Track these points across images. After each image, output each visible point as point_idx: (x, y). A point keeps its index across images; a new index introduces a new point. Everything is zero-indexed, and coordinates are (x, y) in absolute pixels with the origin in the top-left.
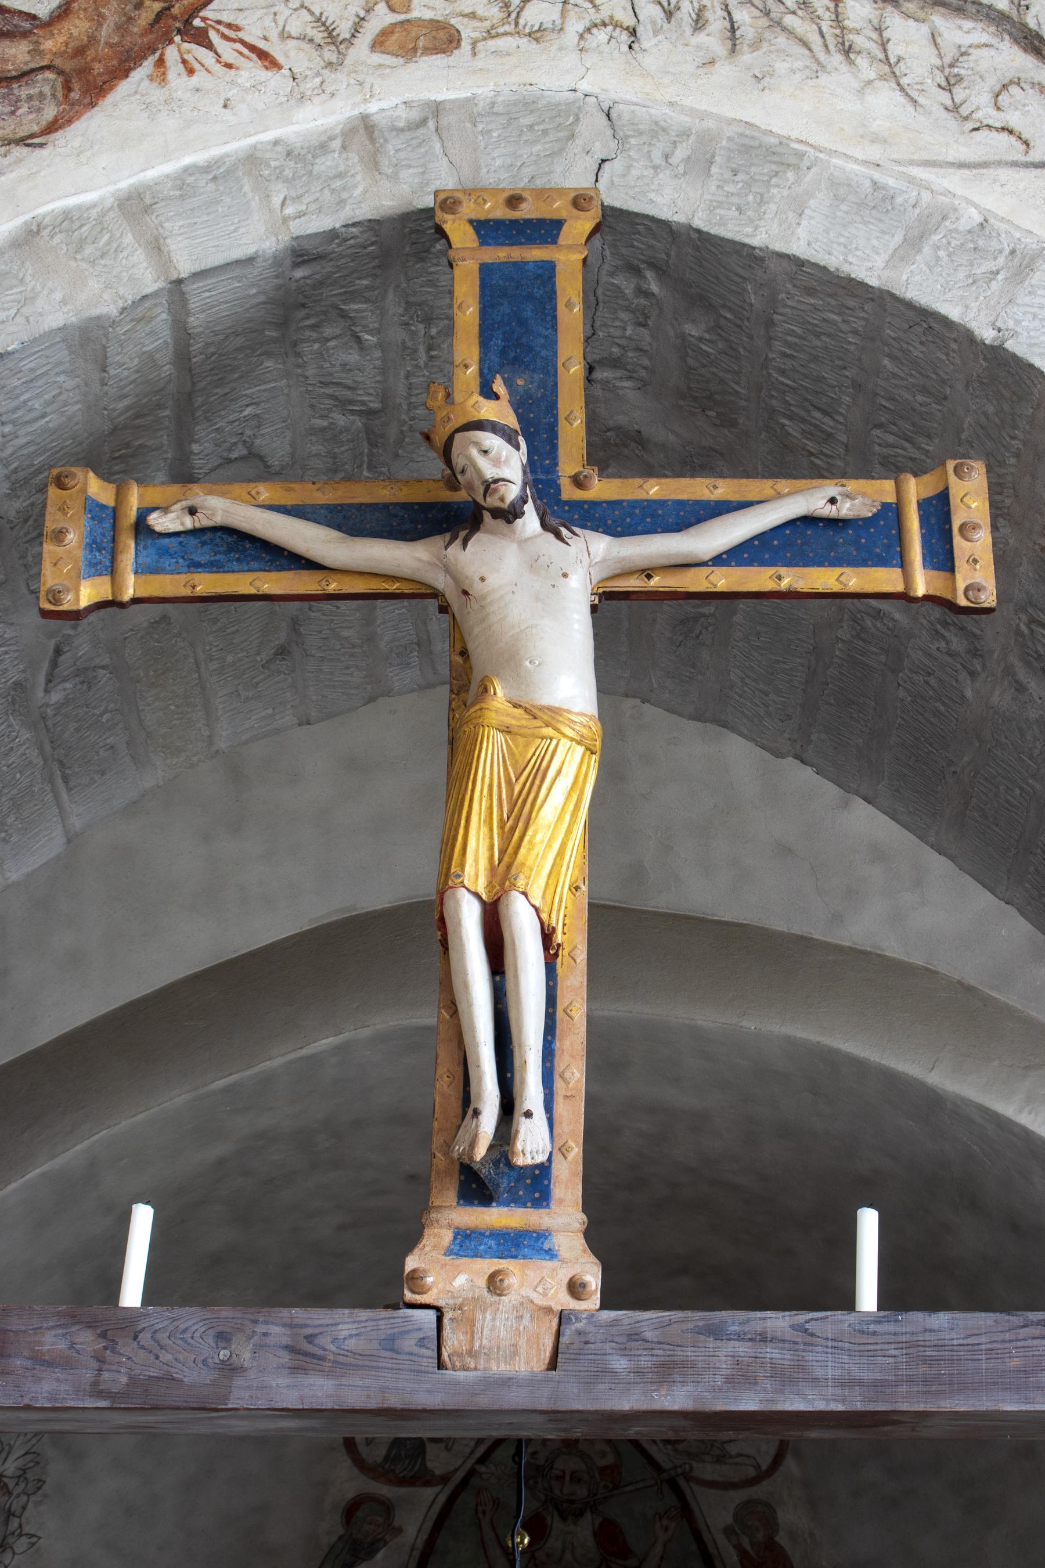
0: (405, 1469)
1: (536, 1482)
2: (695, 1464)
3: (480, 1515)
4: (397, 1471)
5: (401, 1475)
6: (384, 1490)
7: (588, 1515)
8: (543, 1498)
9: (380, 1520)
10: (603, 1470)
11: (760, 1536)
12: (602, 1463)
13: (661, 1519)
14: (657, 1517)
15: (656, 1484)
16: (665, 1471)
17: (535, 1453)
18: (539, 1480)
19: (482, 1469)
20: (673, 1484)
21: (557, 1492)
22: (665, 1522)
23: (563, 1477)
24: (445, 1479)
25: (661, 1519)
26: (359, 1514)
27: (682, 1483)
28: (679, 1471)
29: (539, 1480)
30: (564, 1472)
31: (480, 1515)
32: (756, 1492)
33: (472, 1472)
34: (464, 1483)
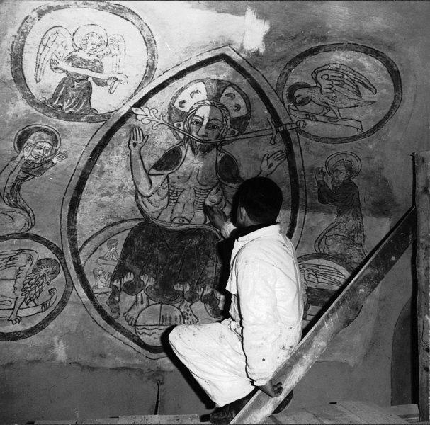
0: (71, 107)
1: (179, 125)
2: (308, 122)
3: (132, 146)
4: (65, 108)
5: (67, 112)
6: (53, 123)
7: (214, 151)
8: (182, 136)
9: (49, 146)
10: (234, 121)
11: (342, 177)
12: (235, 115)
13: (268, 158)
14: (266, 158)
15: (273, 134)
16: (282, 125)
17: (184, 102)
18: (182, 123)
19: (139, 111)
20: (286, 136)
21: (194, 134)
22: (270, 161)
23: (202, 123)
24: (107, 116)
25: (268, 158)
26: (30, 140)
27: (293, 136)
28: (294, 126)
29: (182, 123)
30: (203, 119)
31: (132, 146)
32: (347, 147)
33: (129, 114)
34: (122, 120)
